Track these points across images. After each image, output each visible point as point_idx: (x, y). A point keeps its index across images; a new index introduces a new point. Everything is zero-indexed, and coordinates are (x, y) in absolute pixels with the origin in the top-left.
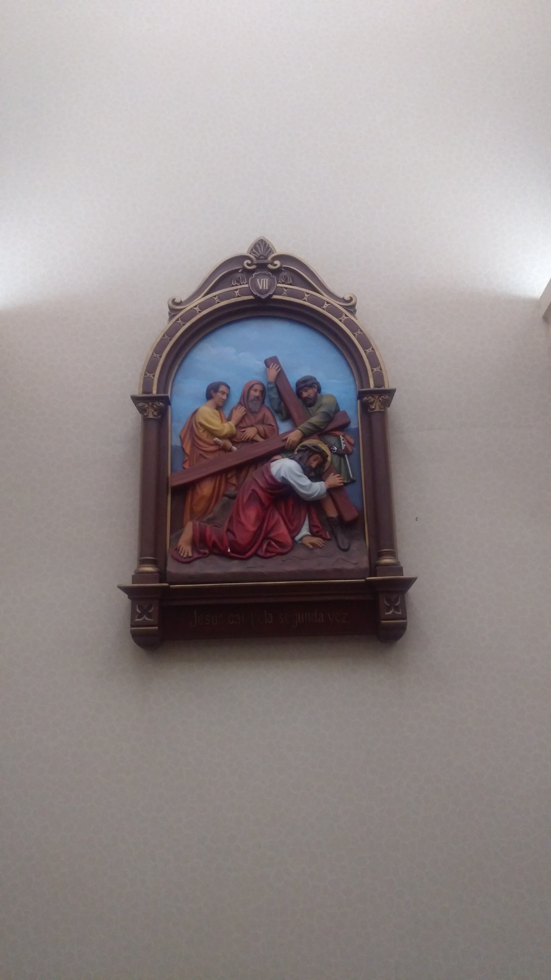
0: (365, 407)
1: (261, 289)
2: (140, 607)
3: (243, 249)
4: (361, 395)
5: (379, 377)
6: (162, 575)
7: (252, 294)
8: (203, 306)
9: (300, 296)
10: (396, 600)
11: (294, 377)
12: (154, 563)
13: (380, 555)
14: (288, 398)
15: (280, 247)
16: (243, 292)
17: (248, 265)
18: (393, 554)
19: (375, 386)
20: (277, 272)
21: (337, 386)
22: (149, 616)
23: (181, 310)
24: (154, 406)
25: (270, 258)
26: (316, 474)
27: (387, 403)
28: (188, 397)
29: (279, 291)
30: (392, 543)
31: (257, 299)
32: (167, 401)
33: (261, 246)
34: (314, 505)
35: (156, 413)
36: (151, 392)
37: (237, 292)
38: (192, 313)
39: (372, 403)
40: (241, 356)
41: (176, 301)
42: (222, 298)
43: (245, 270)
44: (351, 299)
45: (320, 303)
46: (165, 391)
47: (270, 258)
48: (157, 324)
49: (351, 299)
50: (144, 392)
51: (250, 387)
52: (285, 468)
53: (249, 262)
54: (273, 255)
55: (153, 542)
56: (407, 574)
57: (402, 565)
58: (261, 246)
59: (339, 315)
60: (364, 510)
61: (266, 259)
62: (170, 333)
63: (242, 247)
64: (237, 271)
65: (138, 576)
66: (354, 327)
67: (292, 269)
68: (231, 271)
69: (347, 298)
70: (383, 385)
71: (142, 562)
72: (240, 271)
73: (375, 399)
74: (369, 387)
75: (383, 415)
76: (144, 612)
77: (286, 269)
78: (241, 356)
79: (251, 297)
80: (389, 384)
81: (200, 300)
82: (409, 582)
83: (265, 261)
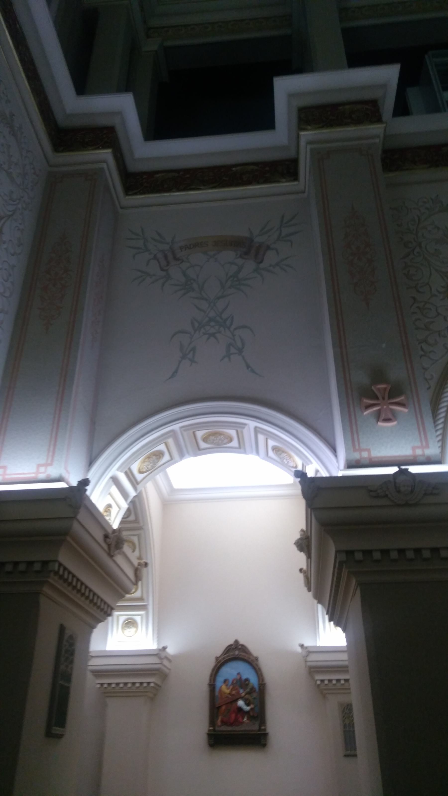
0: (259, 687)
1: (236, 653)
4: (259, 684)
6: (214, 730)
8: (223, 658)
11: (244, 677)
14: (242, 683)
15: (242, 642)
20: (240, 649)
21: (254, 681)
24: (212, 687)
26: (248, 705)
28: (219, 682)
29: (240, 655)
32: (215, 685)
33: (236, 642)
34: (248, 713)
40: (231, 671)
42: (228, 656)
48: (212, 663)
51: (233, 680)
52: (241, 703)
55: (212, 722)
58: (236, 642)
60: (259, 715)
63: (231, 642)
65: (210, 730)
68: (229, 649)
71: (210, 727)
78: (231, 671)
81: (222, 657)
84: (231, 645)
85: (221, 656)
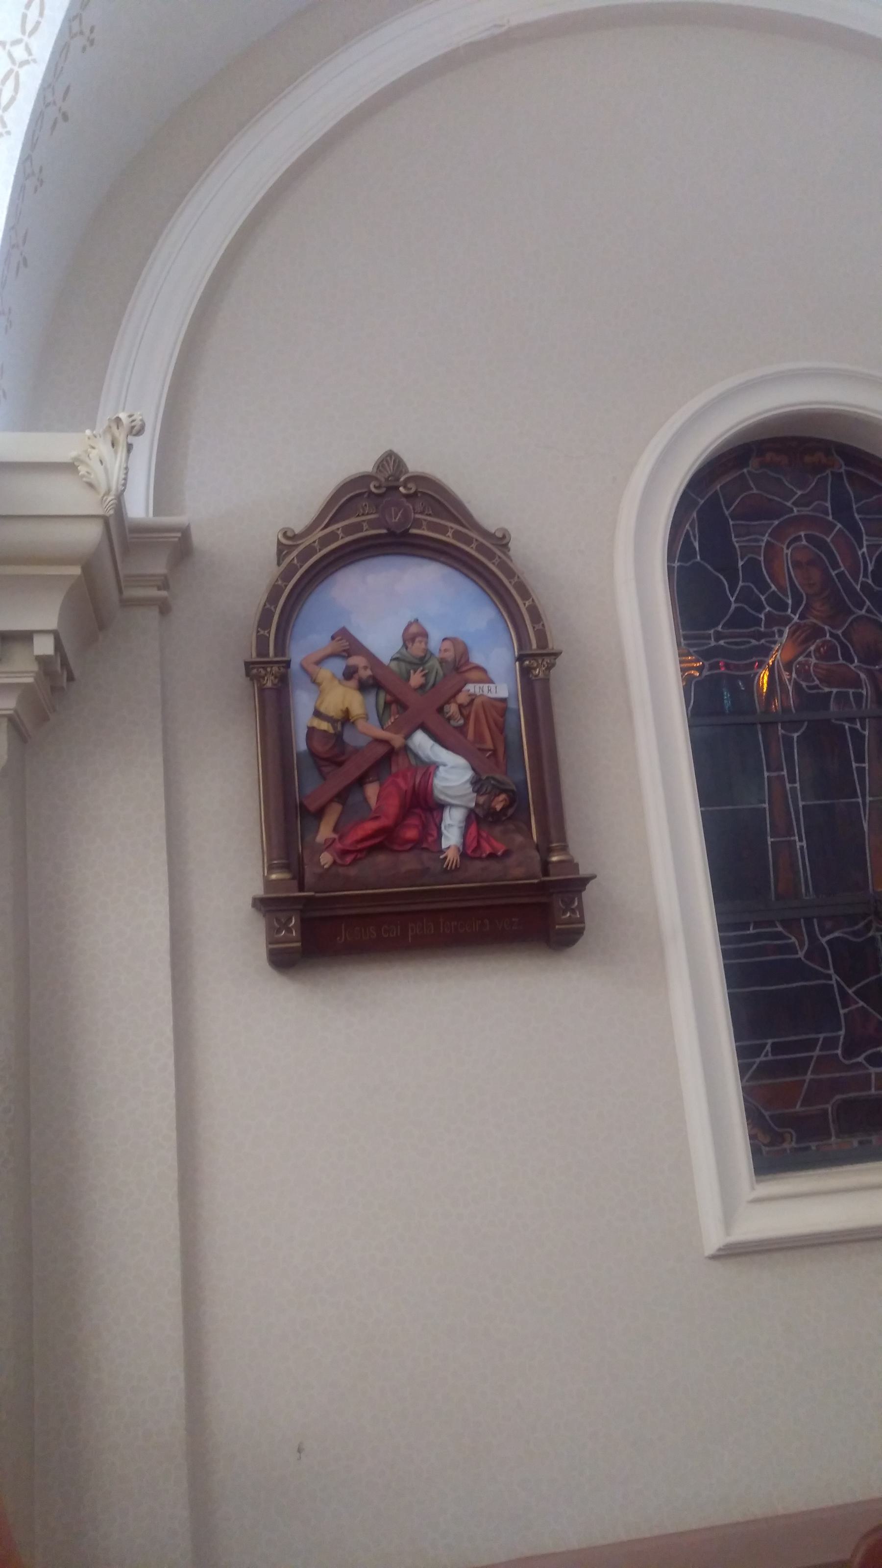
2: (278, 920)
3: (367, 466)
4: (520, 658)
5: (542, 636)
7: (385, 528)
8: (324, 541)
9: (444, 530)
10: (573, 902)
12: (286, 867)
13: (550, 851)
15: (415, 465)
16: (372, 524)
17: (375, 487)
18: (564, 849)
19: (538, 647)
22: (289, 930)
23: (298, 545)
25: (402, 479)
27: (550, 667)
30: (563, 838)
31: (391, 533)
33: (391, 461)
35: (277, 680)
36: (267, 655)
37: (366, 522)
38: (309, 551)
39: (535, 669)
41: (289, 534)
42: (347, 530)
43: (371, 493)
44: (504, 537)
45: (469, 541)
46: (283, 655)
47: (402, 479)
49: (504, 537)
50: (259, 655)
53: (377, 485)
54: (406, 476)
56: (583, 872)
57: (575, 861)
58: (391, 461)
59: (491, 556)
61: (398, 479)
62: (286, 576)
64: (363, 493)
65: (268, 884)
66: (510, 573)
67: (433, 496)
69: (499, 535)
70: (546, 646)
72: (366, 495)
73: (537, 660)
74: (531, 648)
75: (546, 681)
76: (285, 926)
77: (424, 494)
79: (384, 531)
80: (554, 644)
81: (319, 534)
82: (584, 882)
83: (396, 484)
84: (364, 479)
85: (310, 529)
